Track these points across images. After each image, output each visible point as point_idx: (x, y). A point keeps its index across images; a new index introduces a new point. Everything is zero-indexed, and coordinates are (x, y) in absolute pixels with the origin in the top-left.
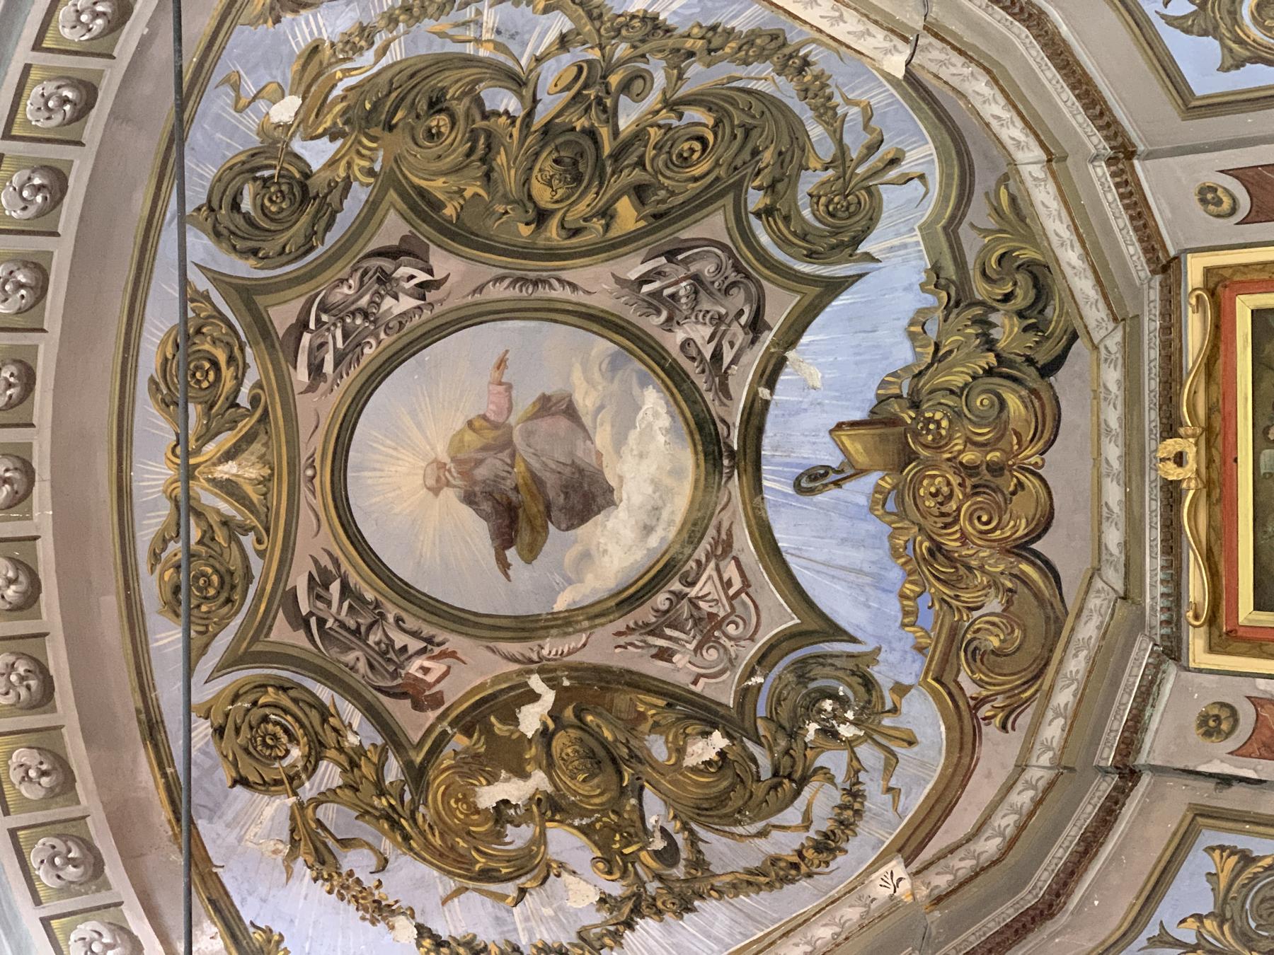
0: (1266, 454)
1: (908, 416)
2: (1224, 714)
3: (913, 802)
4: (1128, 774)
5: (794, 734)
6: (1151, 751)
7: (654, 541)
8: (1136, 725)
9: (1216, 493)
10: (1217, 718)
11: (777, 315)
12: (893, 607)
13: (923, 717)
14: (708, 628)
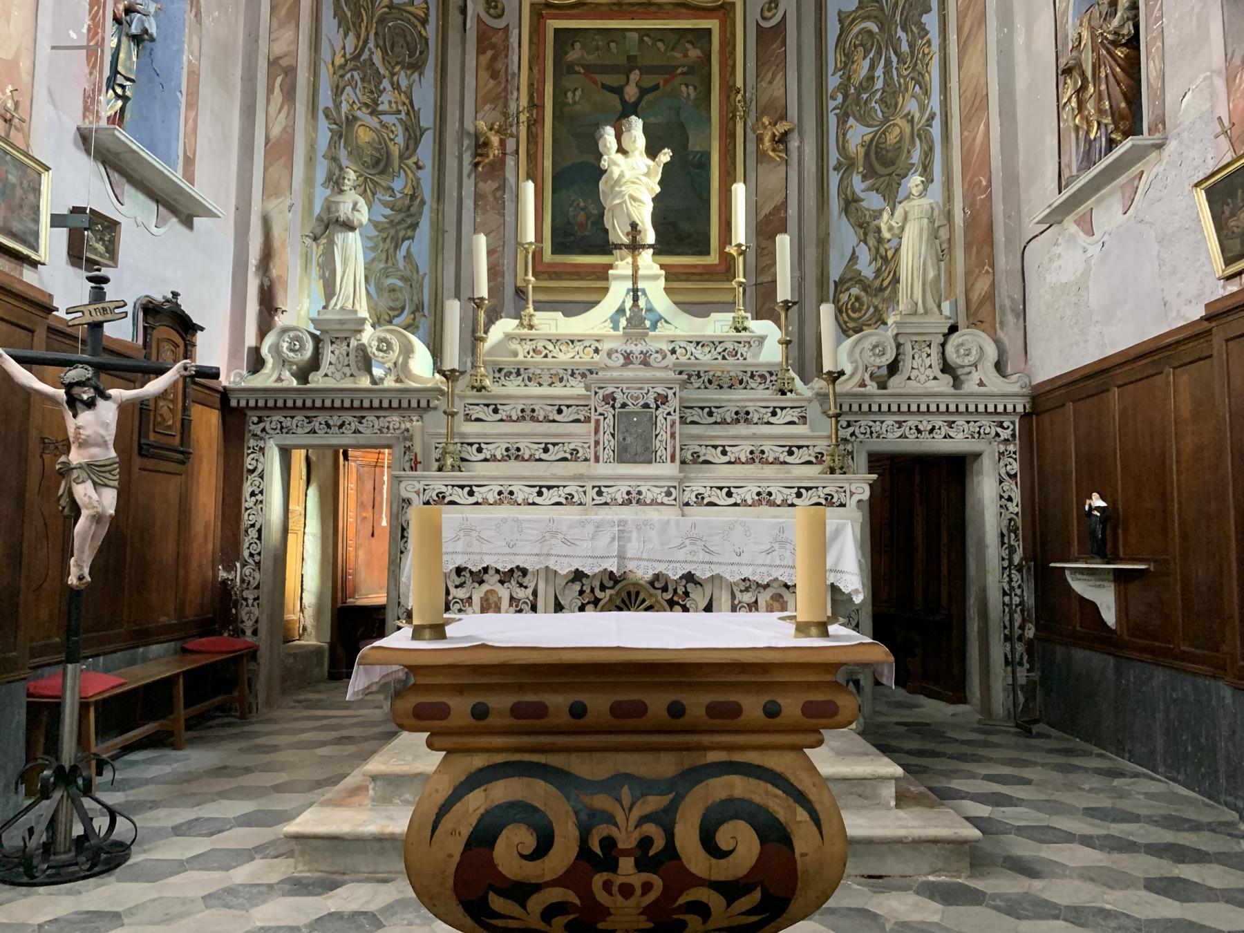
0: (636, 35)
2: (499, 11)
9: (615, 8)
10: (496, 7)
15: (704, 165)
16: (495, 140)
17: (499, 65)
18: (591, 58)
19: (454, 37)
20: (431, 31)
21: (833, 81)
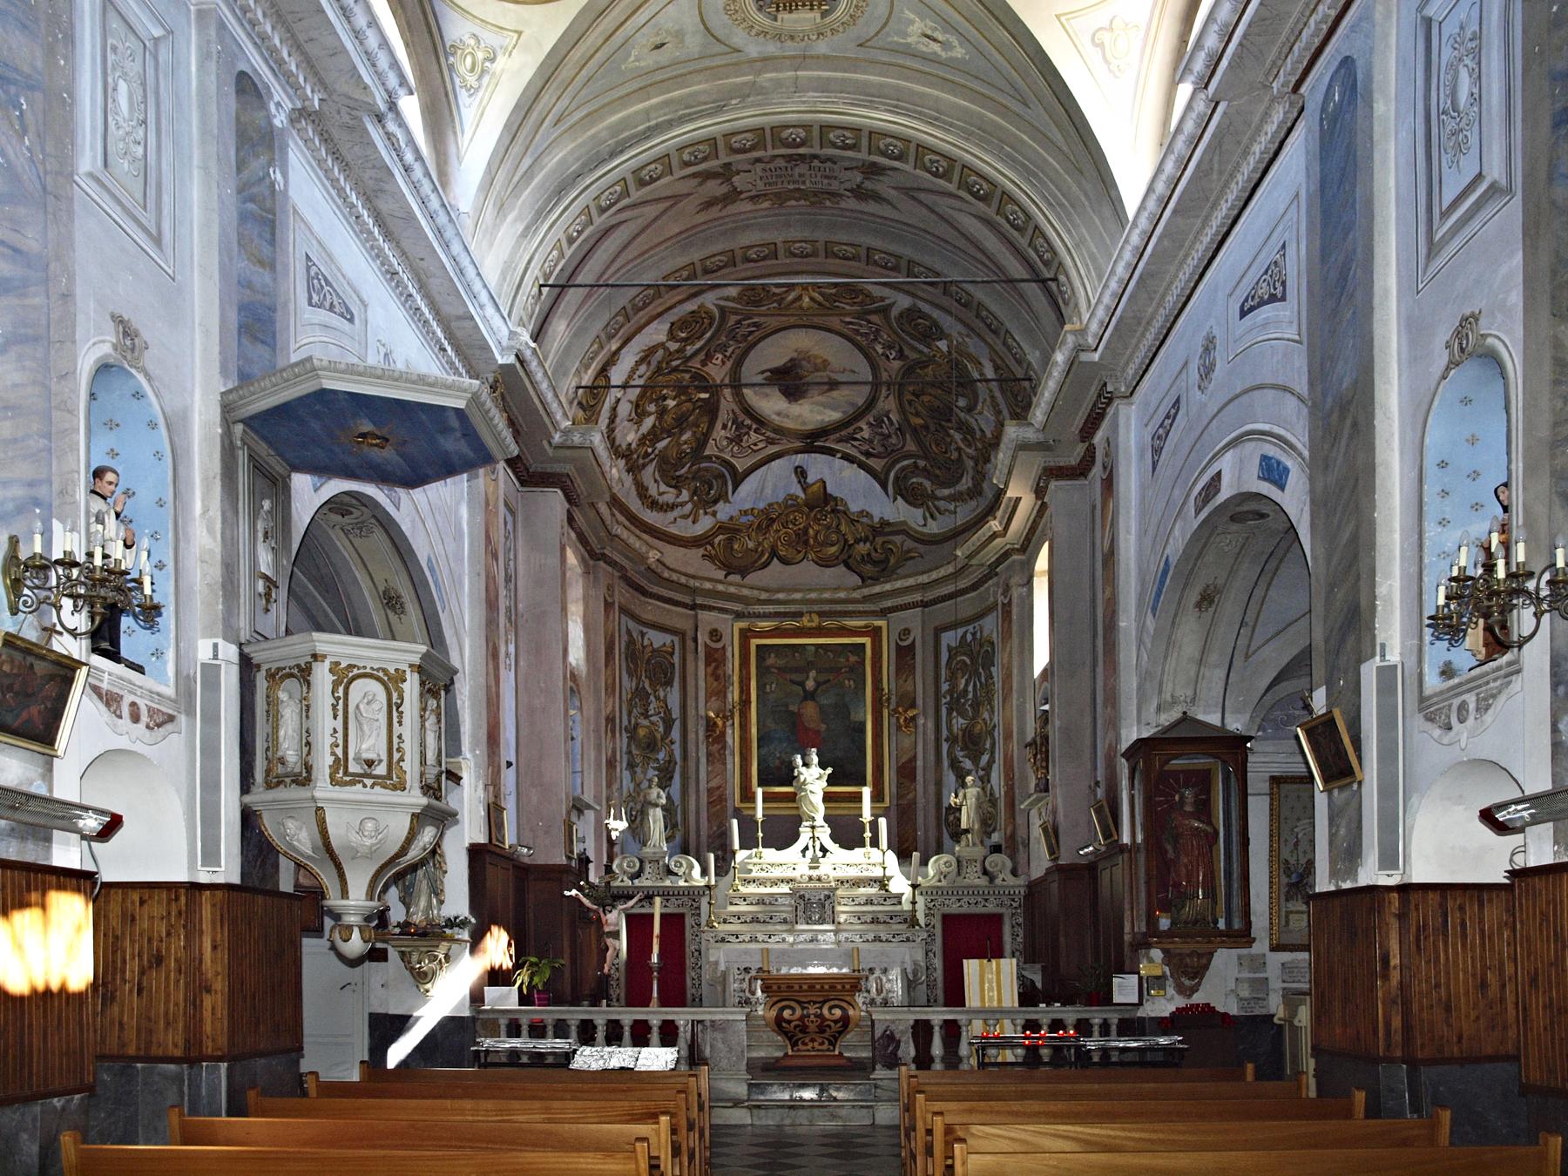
1: (828, 508)
3: (673, 530)
4: (694, 607)
5: (693, 478)
6: (704, 615)
7: (774, 417)
8: (711, 608)
11: (871, 462)
12: (747, 506)
13: (705, 524)
14: (737, 440)
15: (861, 728)
16: (720, 723)
17: (720, 672)
18: (781, 663)
19: (690, 657)
20: (676, 659)
21: (945, 687)
